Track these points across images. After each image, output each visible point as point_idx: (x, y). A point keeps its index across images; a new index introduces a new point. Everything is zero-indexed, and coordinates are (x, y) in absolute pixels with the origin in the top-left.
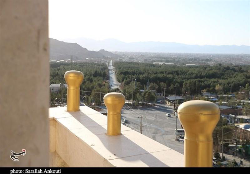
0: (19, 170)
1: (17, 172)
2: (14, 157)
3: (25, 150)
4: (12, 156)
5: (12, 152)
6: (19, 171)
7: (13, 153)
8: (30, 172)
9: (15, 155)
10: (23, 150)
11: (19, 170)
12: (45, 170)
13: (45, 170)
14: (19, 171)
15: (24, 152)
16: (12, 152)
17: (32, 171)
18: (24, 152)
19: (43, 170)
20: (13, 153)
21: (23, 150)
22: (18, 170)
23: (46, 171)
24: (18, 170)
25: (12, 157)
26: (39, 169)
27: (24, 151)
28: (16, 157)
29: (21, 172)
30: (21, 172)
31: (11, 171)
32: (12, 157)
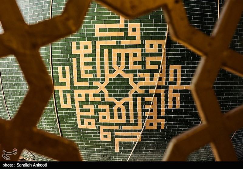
0: (10, 164)
1: (8, 165)
2: (6, 156)
3: (16, 150)
4: (4, 155)
5: (4, 151)
6: (10, 165)
7: (5, 152)
8: (21, 165)
9: (6, 155)
10: (15, 150)
11: (10, 164)
12: (34, 164)
13: (34, 164)
14: (10, 165)
15: (16, 152)
16: (4, 151)
17: (23, 165)
18: (16, 152)
19: (15, 163)
20: (5, 152)
21: (15, 150)
22: (9, 164)
23: (35, 165)
24: (9, 164)
25: (4, 157)
26: (28, 163)
27: (15, 151)
28: (8, 156)
29: (12, 165)
30: (12, 165)
31: (3, 165)
32: (4, 157)
